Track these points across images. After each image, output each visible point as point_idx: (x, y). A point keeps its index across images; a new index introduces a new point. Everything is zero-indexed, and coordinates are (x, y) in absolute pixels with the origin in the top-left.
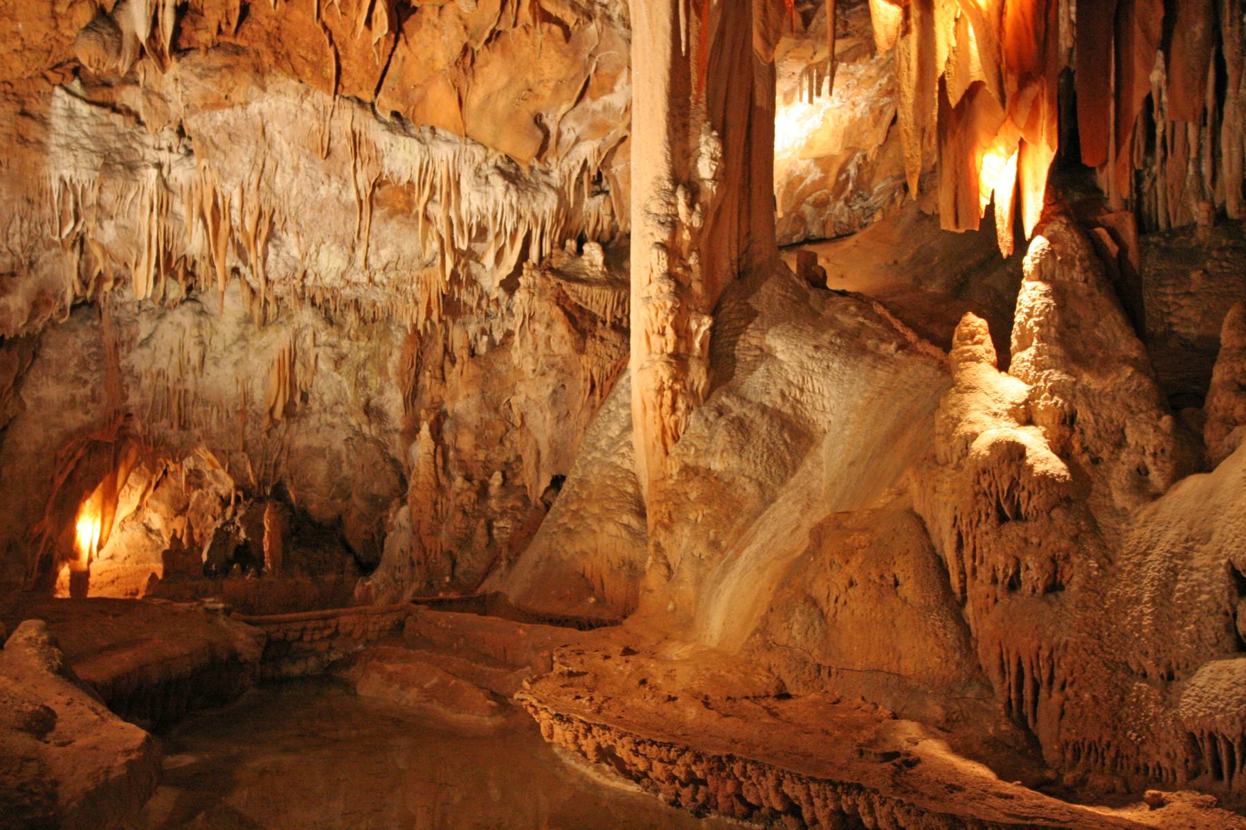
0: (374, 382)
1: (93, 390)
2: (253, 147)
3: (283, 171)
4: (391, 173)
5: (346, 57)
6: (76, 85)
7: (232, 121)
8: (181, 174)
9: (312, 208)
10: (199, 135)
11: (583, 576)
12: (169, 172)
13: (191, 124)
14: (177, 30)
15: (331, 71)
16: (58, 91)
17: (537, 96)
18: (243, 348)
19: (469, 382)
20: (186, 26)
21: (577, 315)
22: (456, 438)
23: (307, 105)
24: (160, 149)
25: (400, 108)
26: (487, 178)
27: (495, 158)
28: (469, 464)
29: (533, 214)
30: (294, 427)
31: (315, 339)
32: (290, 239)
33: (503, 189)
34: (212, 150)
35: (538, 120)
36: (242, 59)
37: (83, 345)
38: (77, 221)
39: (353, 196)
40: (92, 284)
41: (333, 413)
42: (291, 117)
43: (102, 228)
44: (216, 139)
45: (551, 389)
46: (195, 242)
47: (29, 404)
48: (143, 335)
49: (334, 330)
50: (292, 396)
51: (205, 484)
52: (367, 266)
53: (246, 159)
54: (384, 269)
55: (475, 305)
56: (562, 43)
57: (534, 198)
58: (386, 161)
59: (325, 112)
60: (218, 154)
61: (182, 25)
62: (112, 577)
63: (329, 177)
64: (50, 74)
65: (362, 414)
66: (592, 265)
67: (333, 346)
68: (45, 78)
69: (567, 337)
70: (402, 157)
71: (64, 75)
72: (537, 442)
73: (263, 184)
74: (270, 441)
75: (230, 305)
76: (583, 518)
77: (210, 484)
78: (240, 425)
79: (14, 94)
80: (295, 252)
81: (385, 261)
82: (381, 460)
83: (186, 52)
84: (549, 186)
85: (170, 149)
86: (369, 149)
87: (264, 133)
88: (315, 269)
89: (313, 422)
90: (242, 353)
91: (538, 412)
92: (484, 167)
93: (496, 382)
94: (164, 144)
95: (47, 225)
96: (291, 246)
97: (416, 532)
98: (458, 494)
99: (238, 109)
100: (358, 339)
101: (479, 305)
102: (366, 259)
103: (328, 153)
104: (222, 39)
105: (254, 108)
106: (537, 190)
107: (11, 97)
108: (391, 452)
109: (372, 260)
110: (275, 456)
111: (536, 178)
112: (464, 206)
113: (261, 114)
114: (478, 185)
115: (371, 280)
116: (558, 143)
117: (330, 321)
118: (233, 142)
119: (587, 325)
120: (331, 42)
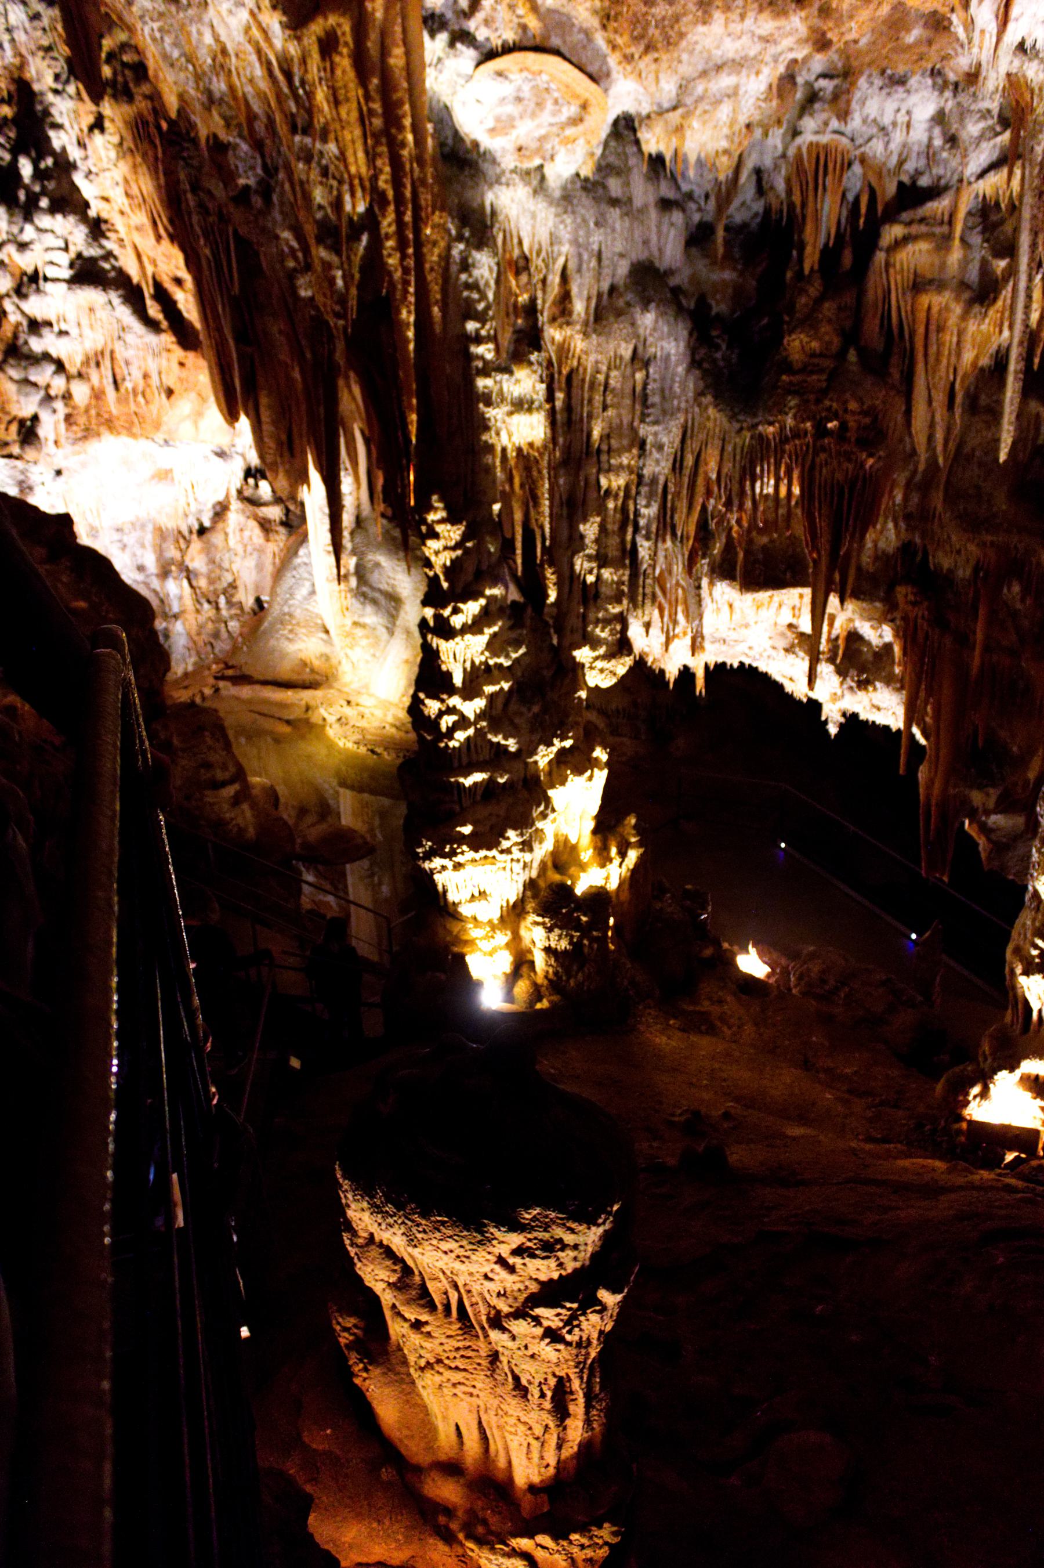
25: (167, 437)
97: (189, 635)
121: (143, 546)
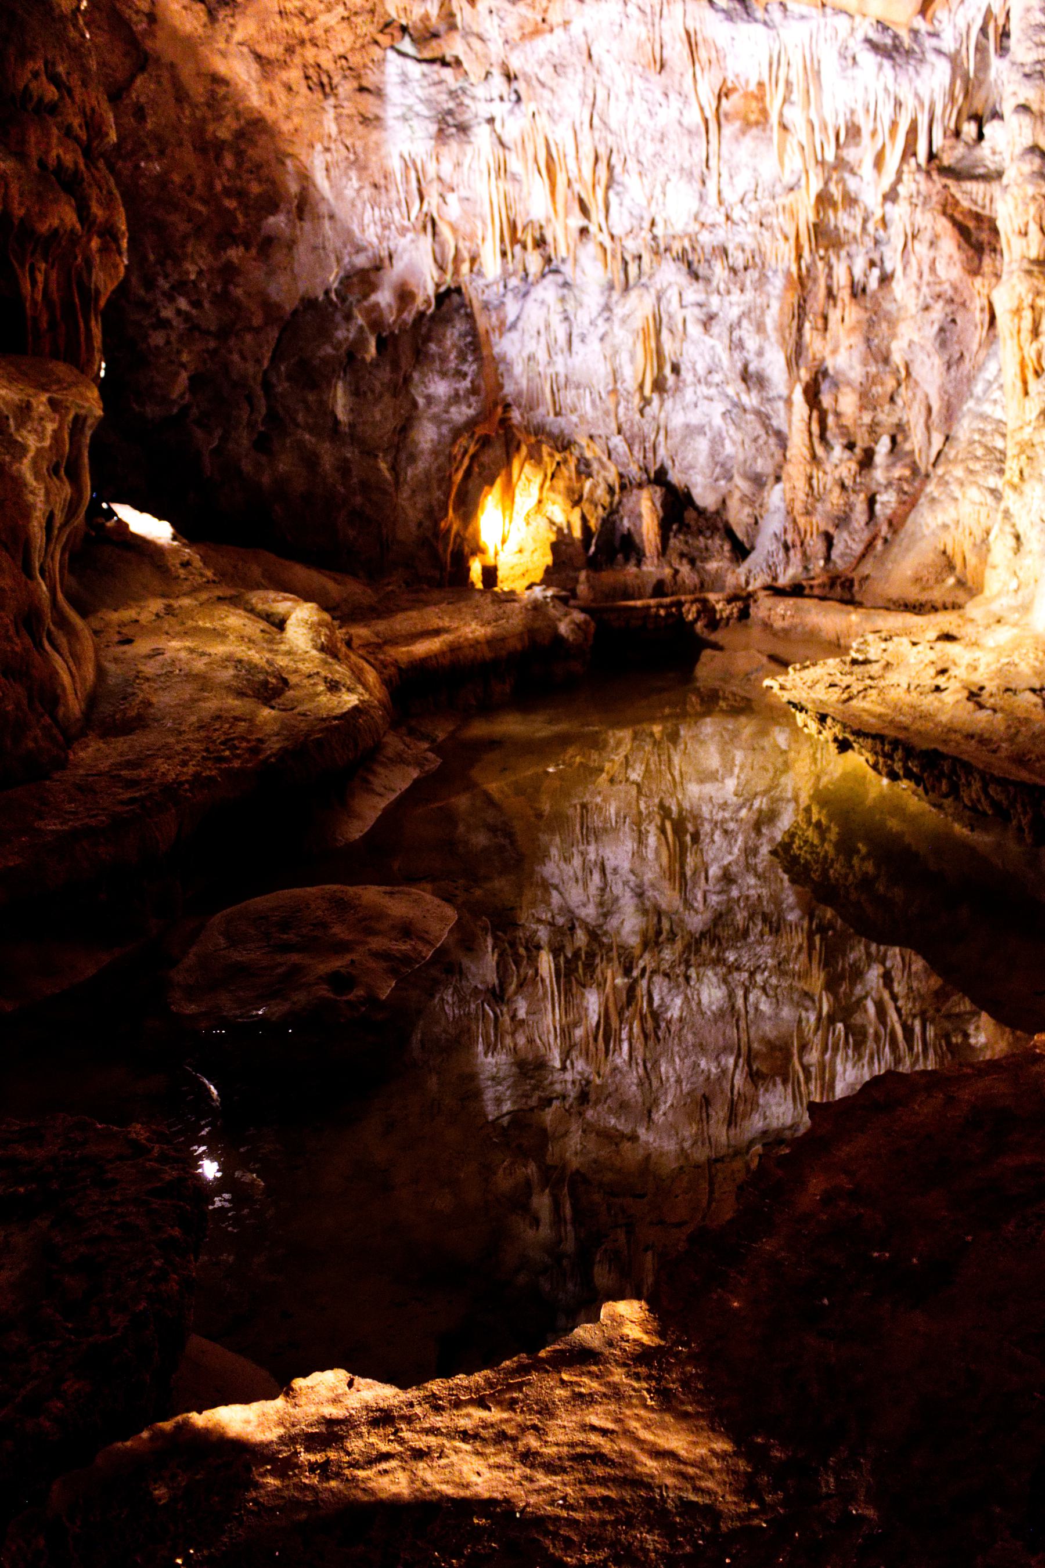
0: (752, 343)
1: (472, 382)
2: (580, 77)
3: (617, 99)
4: (737, 76)
6: (406, 45)
7: (556, 51)
8: (512, 129)
9: (652, 140)
10: (525, 74)
11: (944, 552)
12: (503, 125)
13: (515, 64)
16: (391, 55)
18: (608, 319)
19: (853, 329)
21: (971, 224)
22: (836, 400)
24: (492, 100)
26: (854, 58)
27: (866, 28)
28: (852, 429)
29: (917, 95)
30: (669, 404)
33: (875, 69)
34: (539, 89)
37: (460, 335)
38: (422, 199)
41: (708, 384)
42: (616, 29)
43: (445, 202)
44: (542, 77)
45: (936, 327)
46: (536, 204)
47: (421, 401)
48: (511, 318)
49: (700, 286)
50: (660, 368)
51: (594, 473)
52: (721, 202)
53: (575, 93)
54: (742, 201)
55: (858, 230)
57: (917, 72)
58: (730, 62)
59: (653, 14)
60: (546, 93)
62: (522, 570)
63: (666, 95)
64: (380, 38)
65: (739, 382)
66: (994, 153)
67: (700, 305)
69: (957, 255)
71: (392, 35)
72: (927, 397)
73: (596, 121)
74: (643, 421)
75: (590, 272)
76: (947, 483)
77: (598, 473)
78: (612, 407)
79: (350, 69)
81: (741, 193)
82: (762, 432)
84: (939, 52)
85: (502, 99)
86: (709, 52)
87: (590, 56)
88: (664, 215)
89: (689, 395)
90: (607, 326)
91: (925, 358)
92: (851, 43)
93: (884, 325)
94: (495, 95)
95: (395, 211)
96: (634, 191)
98: (836, 466)
99: (559, 32)
100: (729, 292)
101: (864, 229)
102: (719, 193)
103: (662, 67)
105: (576, 29)
106: (922, 61)
107: (348, 73)
108: (775, 423)
109: (727, 194)
110: (653, 437)
111: (921, 45)
114: (844, 69)
117: (695, 276)
118: (559, 75)
119: (984, 236)
121: (760, 328)
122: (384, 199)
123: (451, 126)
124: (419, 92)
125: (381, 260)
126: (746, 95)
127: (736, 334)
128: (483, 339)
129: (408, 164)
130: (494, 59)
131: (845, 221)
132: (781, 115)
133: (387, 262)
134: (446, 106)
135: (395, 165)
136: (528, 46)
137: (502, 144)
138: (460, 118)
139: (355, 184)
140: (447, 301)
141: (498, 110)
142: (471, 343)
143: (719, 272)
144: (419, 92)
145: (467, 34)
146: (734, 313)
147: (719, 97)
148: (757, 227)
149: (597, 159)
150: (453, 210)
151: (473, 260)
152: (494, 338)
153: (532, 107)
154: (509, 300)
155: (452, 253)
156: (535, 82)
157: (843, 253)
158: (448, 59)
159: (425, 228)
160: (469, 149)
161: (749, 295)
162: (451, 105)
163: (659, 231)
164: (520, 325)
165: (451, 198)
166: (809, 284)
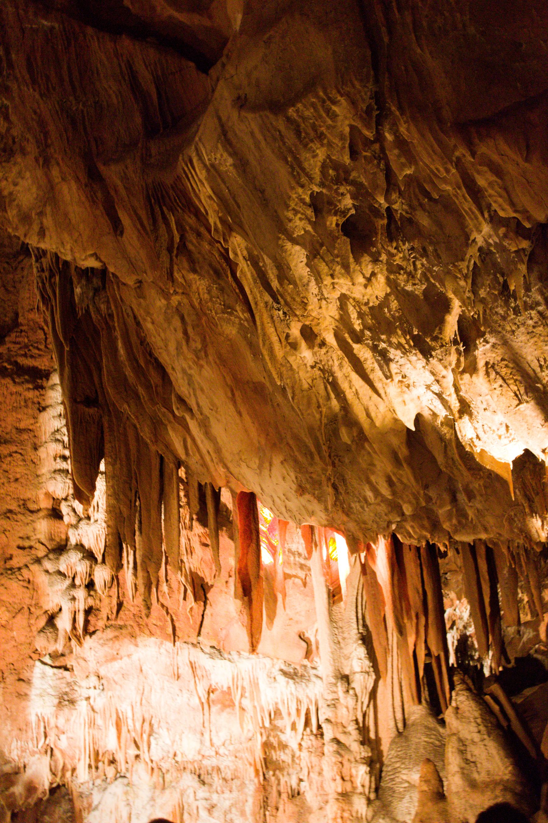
5: (178, 620)
8: (99, 703)
13: (102, 673)
14: (87, 622)
15: (170, 630)
16: (38, 663)
17: (297, 622)
20: (91, 618)
23: (162, 650)
25: (214, 644)
29: (307, 697)
31: (195, 796)
32: (163, 732)
33: (285, 684)
34: (114, 685)
35: (301, 637)
36: (124, 631)
38: (46, 737)
39: (197, 701)
40: (60, 774)
44: (116, 678)
46: (110, 742)
49: (206, 788)
52: (212, 745)
55: (290, 761)
56: (303, 588)
57: (307, 686)
58: (213, 677)
60: (118, 687)
61: (90, 618)
67: (206, 799)
68: (31, 657)
70: (220, 672)
73: (144, 701)
80: (168, 742)
81: (223, 740)
83: (94, 632)
85: (95, 688)
87: (141, 670)
92: (273, 670)
94: (92, 685)
99: (125, 659)
102: (211, 740)
103: (178, 677)
104: (110, 622)
105: (135, 657)
109: (215, 740)
111: (308, 673)
112: (263, 698)
113: (139, 660)
115: (217, 753)
116: (317, 648)
117: (204, 783)
120: (168, 613)
122: (24, 736)
123: (66, 701)
124: (51, 682)
125: (19, 768)
126: (223, 692)
127: (229, 817)
128: (77, 814)
129: (40, 719)
130: (91, 670)
131: (283, 757)
132: (240, 703)
133: (22, 770)
134: (64, 690)
135: (33, 719)
136: (109, 665)
137: (93, 710)
138: (71, 697)
139: (9, 728)
140: (58, 791)
141: (92, 693)
142: (70, 817)
143: (217, 782)
144: (51, 682)
145: (78, 657)
146: (227, 804)
147: (209, 693)
148: (233, 758)
149: (144, 721)
150: (63, 743)
151: (74, 770)
152: (85, 814)
153: (110, 693)
154: (95, 792)
155: (60, 767)
156: (112, 682)
157: (285, 773)
158: (68, 666)
159: (46, 752)
160: (74, 712)
161: (235, 794)
162: (67, 690)
163: (178, 758)
164: (100, 807)
165: (63, 737)
166: (269, 788)
